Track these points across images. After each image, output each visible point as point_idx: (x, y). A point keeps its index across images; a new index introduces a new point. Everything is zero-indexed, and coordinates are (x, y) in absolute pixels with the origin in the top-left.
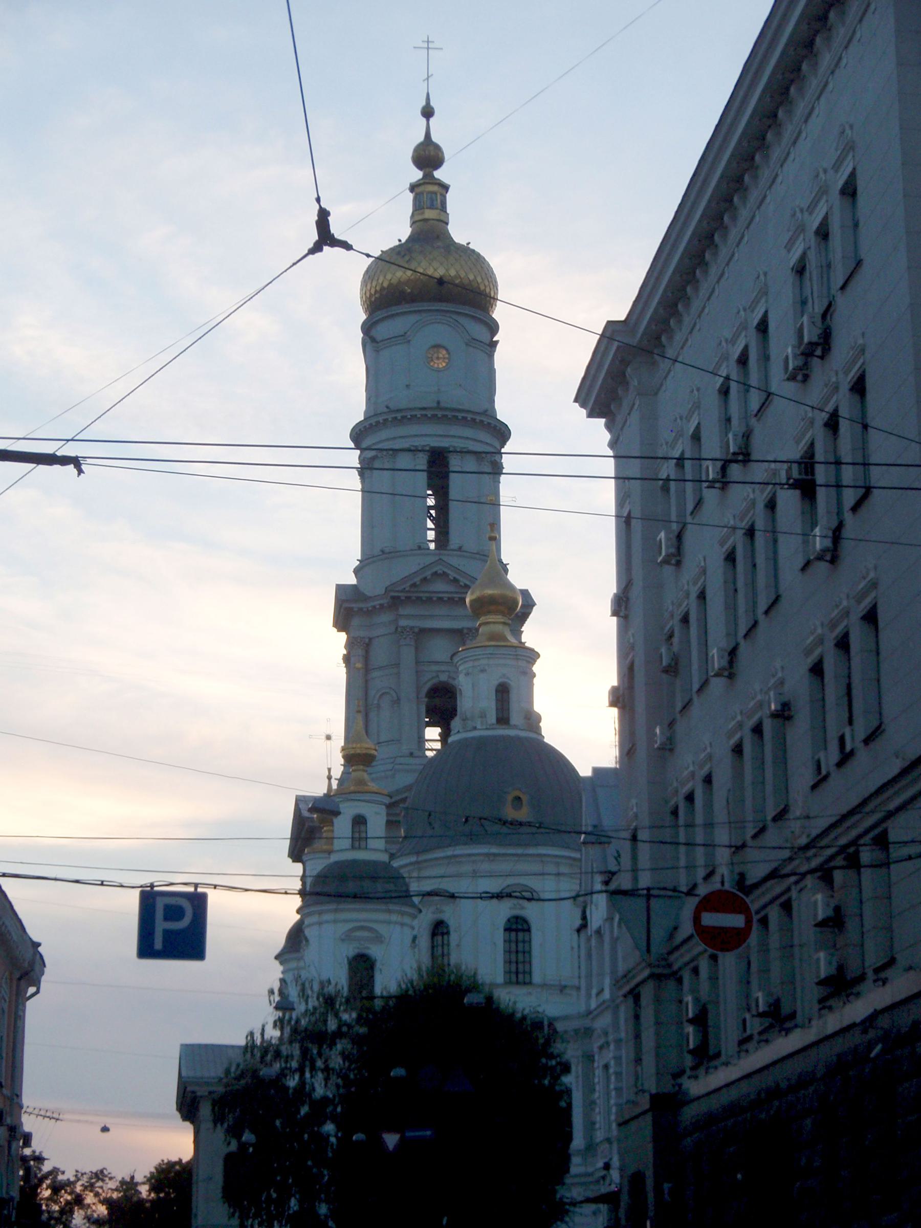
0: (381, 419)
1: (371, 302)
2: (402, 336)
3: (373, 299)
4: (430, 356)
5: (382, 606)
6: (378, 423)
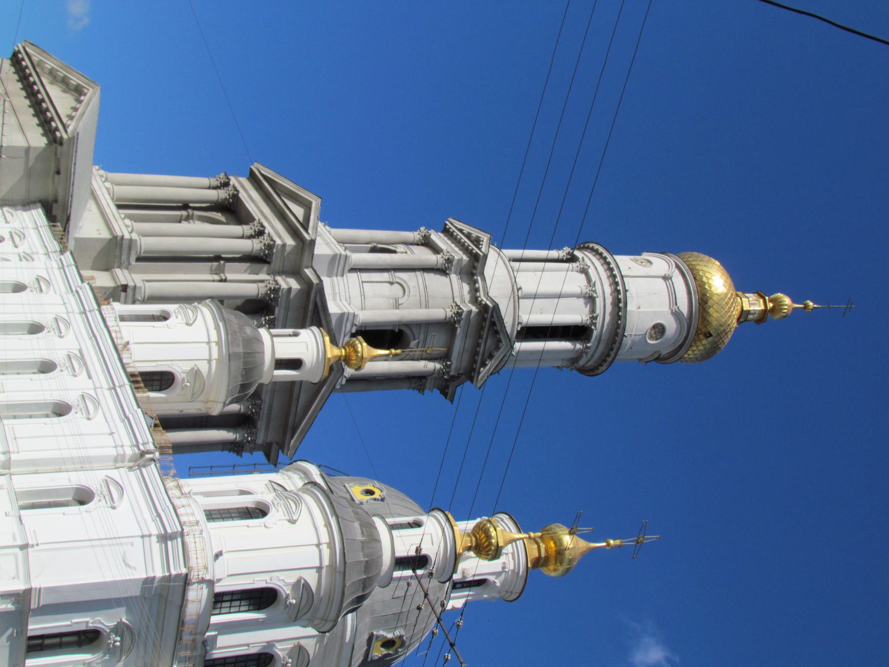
0: (620, 288)
3: (701, 273)
4: (658, 326)
5: (477, 290)
6: (617, 284)
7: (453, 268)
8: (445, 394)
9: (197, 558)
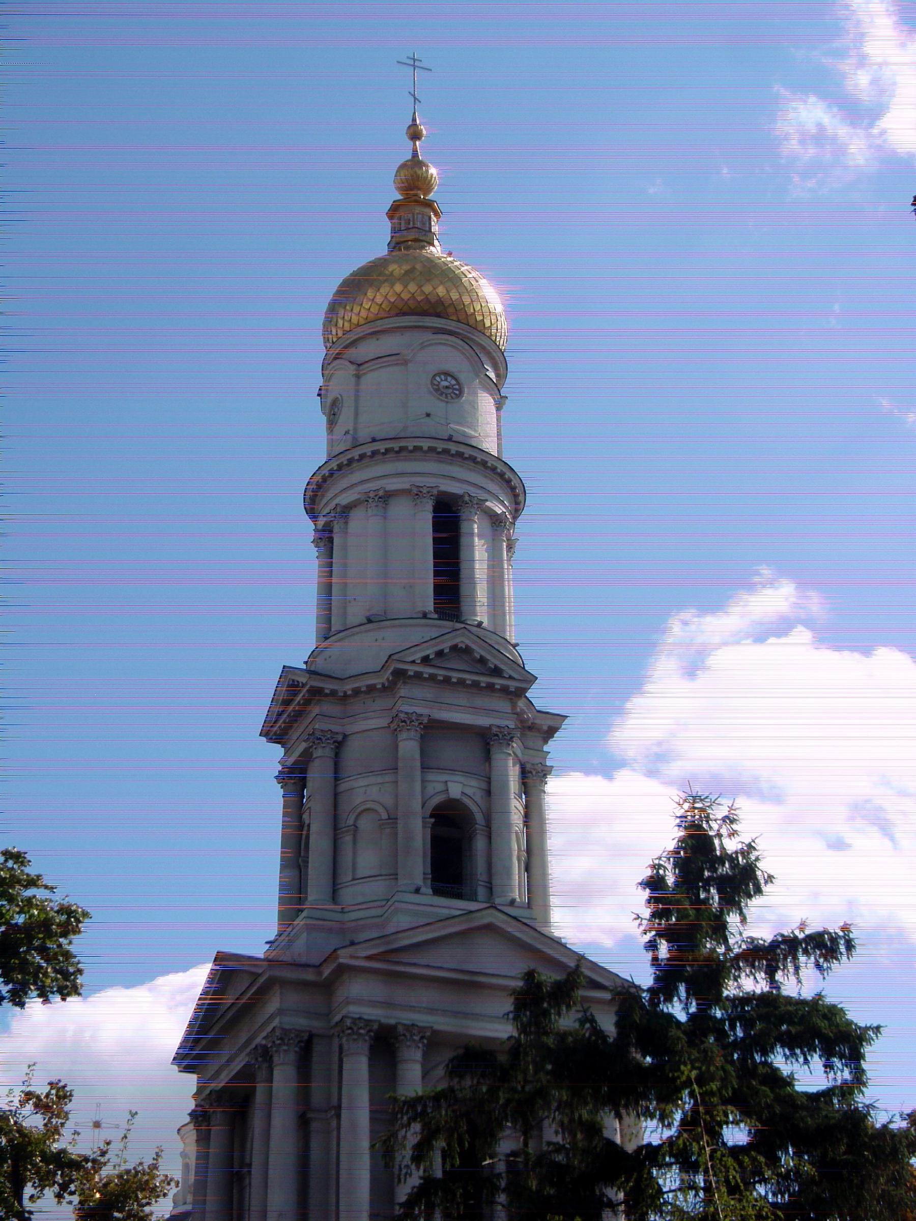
5: (371, 689)
8: (550, 732)
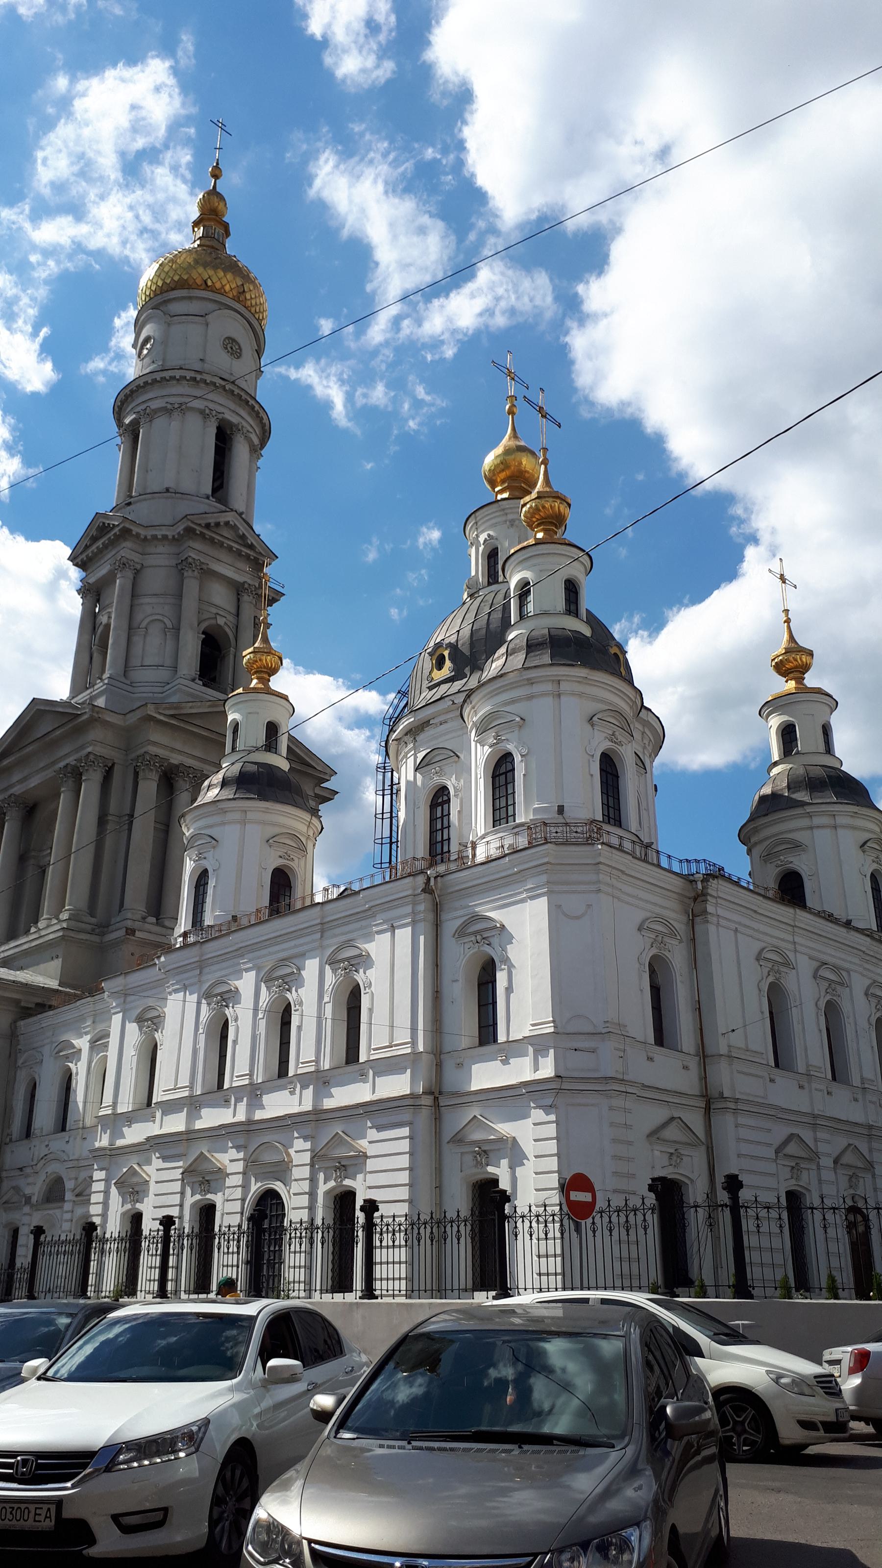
1: (164, 283)
2: (202, 316)
3: (168, 281)
5: (165, 537)
7: (136, 560)
9: (576, 832)
